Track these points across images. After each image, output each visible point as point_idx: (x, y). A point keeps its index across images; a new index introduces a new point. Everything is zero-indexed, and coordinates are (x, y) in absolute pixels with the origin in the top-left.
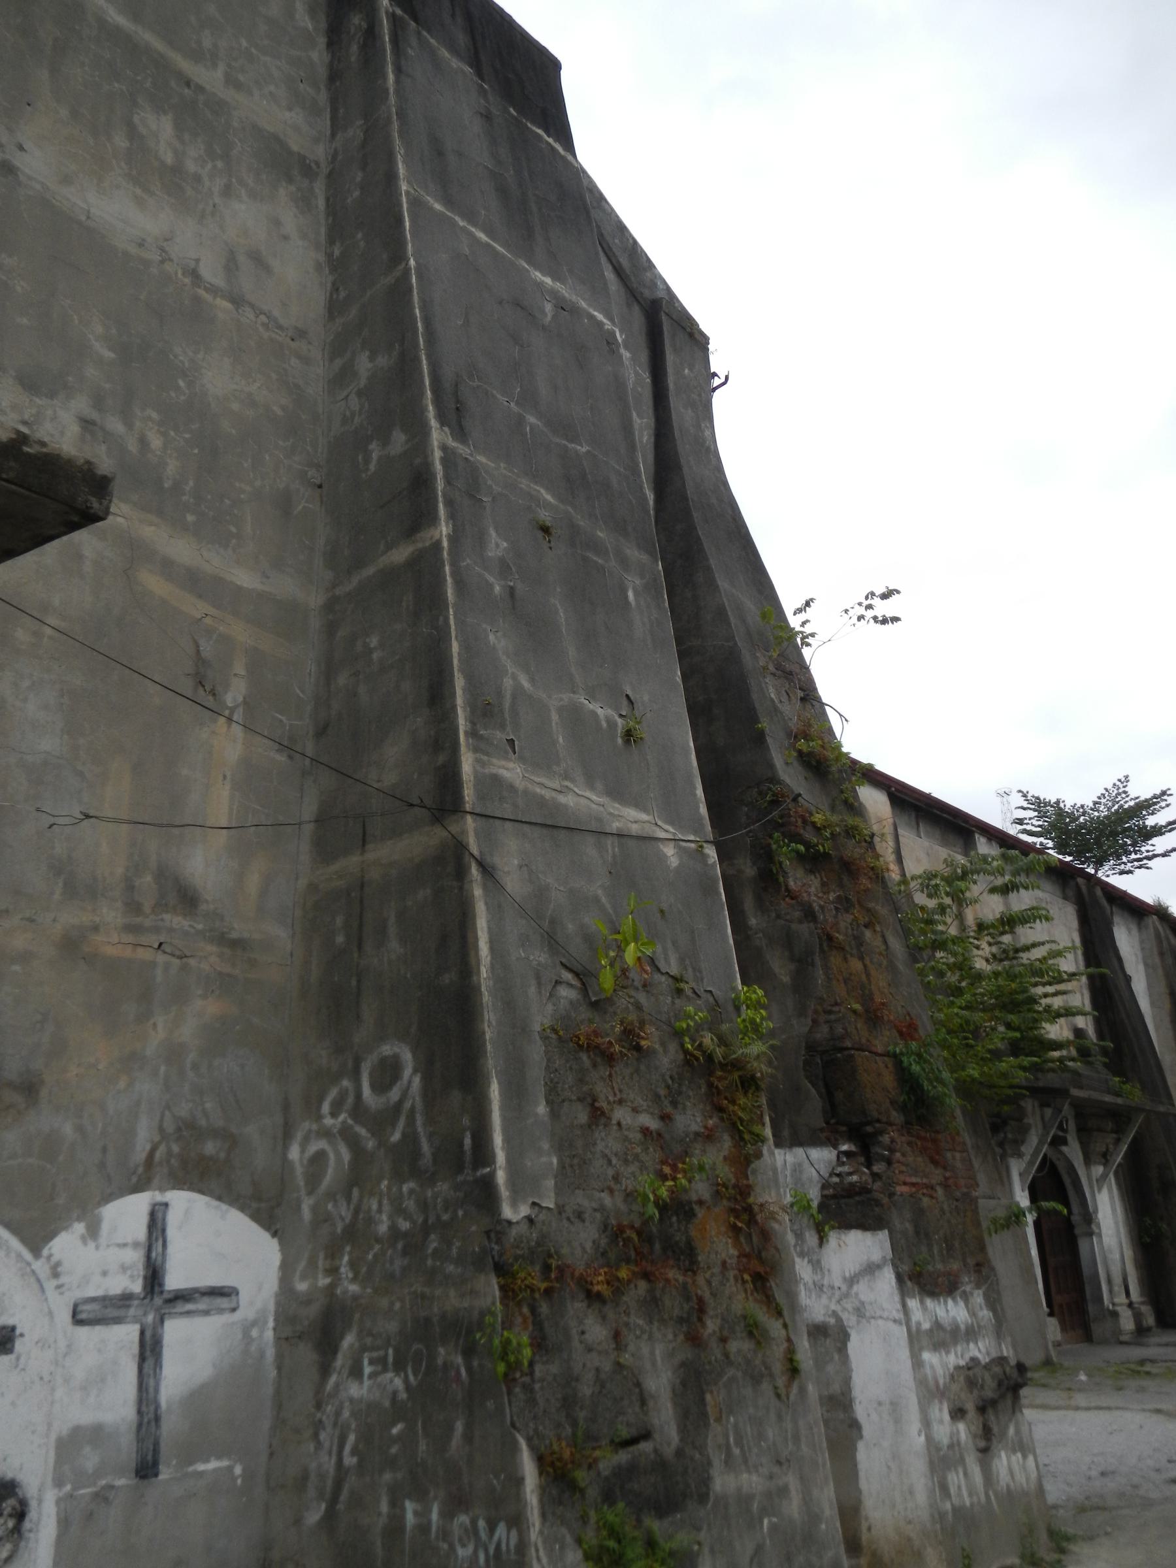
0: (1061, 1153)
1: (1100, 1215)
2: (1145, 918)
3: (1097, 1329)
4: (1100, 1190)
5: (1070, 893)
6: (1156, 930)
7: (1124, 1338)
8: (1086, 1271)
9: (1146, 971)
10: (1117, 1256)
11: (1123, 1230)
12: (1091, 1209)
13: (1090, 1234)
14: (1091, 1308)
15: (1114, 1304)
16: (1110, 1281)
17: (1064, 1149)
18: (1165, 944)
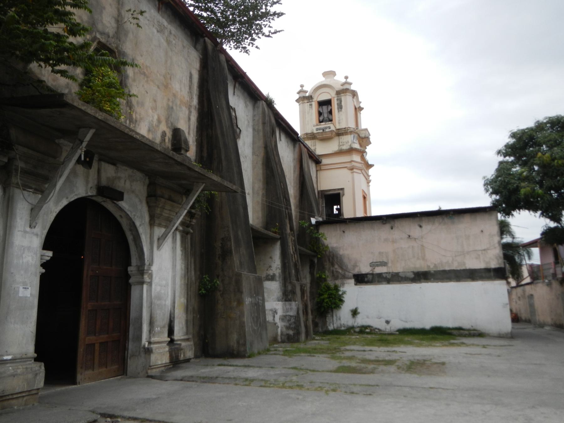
0: (120, 209)
1: (154, 268)
2: (258, 102)
3: (133, 365)
4: (159, 247)
5: (199, 47)
6: (263, 109)
7: (151, 372)
8: (133, 314)
9: (253, 133)
10: (169, 302)
11: (179, 282)
12: (147, 262)
13: (142, 283)
14: (131, 346)
15: (150, 343)
16: (151, 323)
17: (122, 204)
18: (267, 118)
